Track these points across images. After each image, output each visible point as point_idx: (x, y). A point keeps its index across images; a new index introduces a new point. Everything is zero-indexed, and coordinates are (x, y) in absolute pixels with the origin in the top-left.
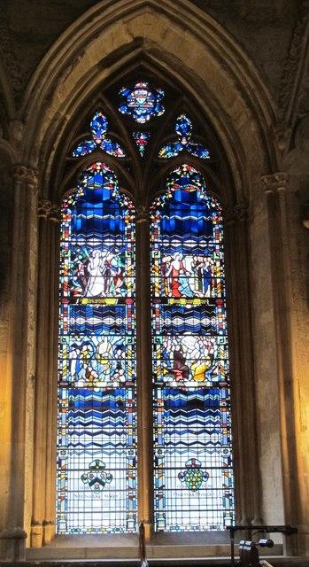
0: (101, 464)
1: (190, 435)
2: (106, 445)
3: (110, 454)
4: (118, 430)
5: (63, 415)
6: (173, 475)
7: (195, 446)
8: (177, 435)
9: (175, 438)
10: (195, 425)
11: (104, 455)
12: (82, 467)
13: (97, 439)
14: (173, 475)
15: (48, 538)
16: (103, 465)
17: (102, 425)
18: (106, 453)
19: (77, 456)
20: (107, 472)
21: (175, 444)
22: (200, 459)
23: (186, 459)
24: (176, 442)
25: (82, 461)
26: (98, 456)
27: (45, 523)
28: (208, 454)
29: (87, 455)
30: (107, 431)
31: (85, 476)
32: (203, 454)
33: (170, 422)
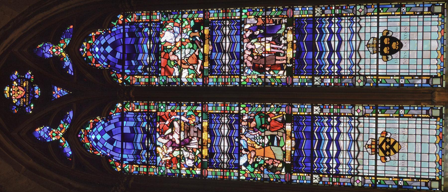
1: (342, 49)
3: (359, 133)
4: (335, 124)
8: (342, 63)
9: (345, 65)
10: (333, 43)
11: (361, 138)
17: (331, 140)
20: (379, 136)
22: (368, 38)
26: (360, 144)
28: (362, 30)
29: (360, 156)
30: (335, 135)
32: (362, 36)
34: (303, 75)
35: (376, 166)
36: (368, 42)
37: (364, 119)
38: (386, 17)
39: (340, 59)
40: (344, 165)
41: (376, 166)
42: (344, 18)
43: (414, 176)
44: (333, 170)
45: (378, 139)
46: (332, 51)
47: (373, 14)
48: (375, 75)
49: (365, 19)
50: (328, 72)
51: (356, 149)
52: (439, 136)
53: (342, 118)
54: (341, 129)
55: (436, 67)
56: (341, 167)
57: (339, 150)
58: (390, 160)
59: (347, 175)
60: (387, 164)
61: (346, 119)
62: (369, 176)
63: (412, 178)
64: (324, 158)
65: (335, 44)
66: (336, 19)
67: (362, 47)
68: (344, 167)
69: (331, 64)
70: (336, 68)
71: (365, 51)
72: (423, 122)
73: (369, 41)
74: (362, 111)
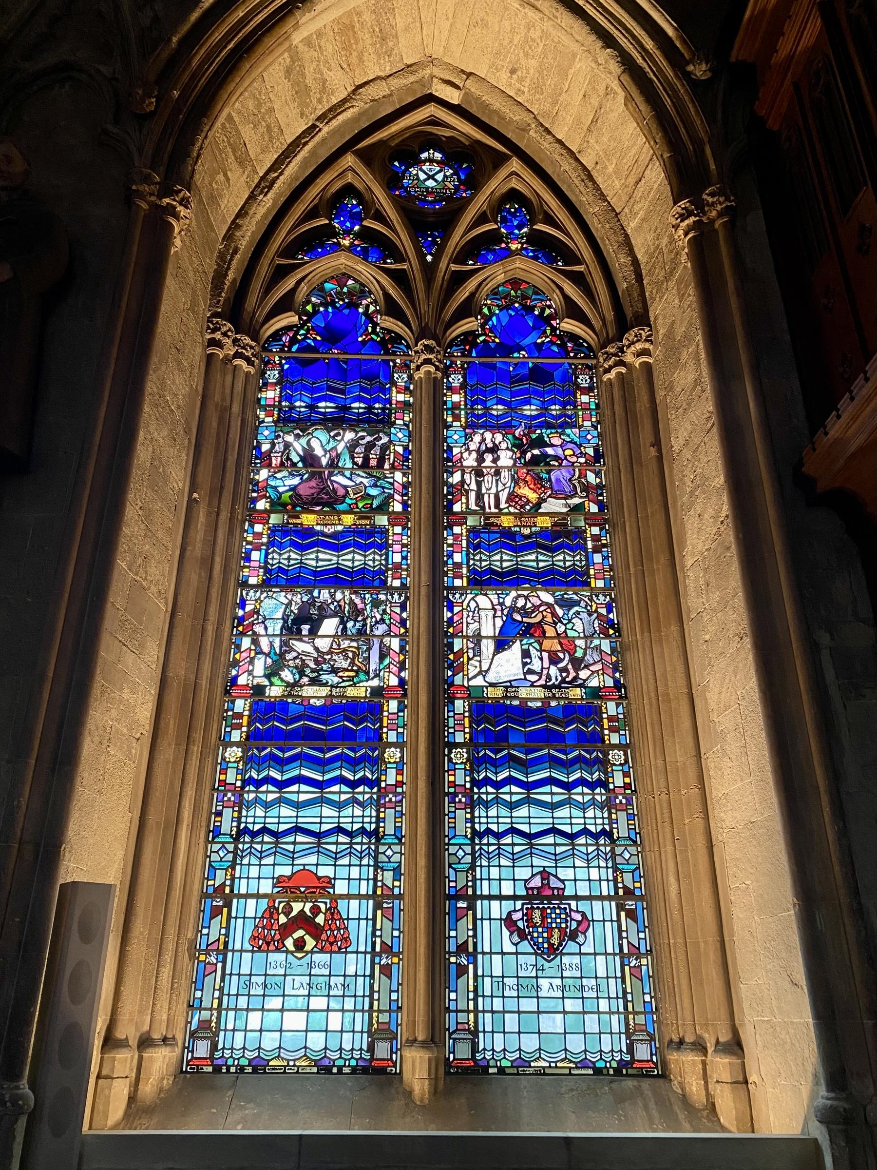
1: (535, 811)
2: (329, 833)
5: (234, 753)
6: (495, 914)
7: (549, 839)
10: (547, 789)
11: (323, 859)
14: (495, 914)
19: (254, 861)
21: (498, 836)
22: (562, 873)
23: (523, 873)
24: (502, 828)
25: (267, 871)
26: (313, 859)
27: (145, 1042)
29: (280, 859)
33: (487, 781)
34: (470, 723)
36: (553, 875)
37: (369, 865)
39: (512, 806)
40: (262, 820)
42: (606, 815)
43: (226, 991)
44: (253, 792)
46: (529, 786)
47: (620, 885)
48: (474, 891)
49: (607, 867)
50: (481, 778)
51: (299, 847)
52: (325, 1056)
53: (374, 814)
54: (348, 811)
55: (499, 1047)
56: (260, 812)
57: (298, 806)
59: (238, 827)
62: (233, 879)
63: (221, 989)
64: (282, 772)
65: (544, 794)
66: (604, 798)
67: (536, 861)
68: (257, 820)
69: (498, 785)
71: (532, 866)
72: (359, 1015)
73: (556, 876)
74: (390, 862)
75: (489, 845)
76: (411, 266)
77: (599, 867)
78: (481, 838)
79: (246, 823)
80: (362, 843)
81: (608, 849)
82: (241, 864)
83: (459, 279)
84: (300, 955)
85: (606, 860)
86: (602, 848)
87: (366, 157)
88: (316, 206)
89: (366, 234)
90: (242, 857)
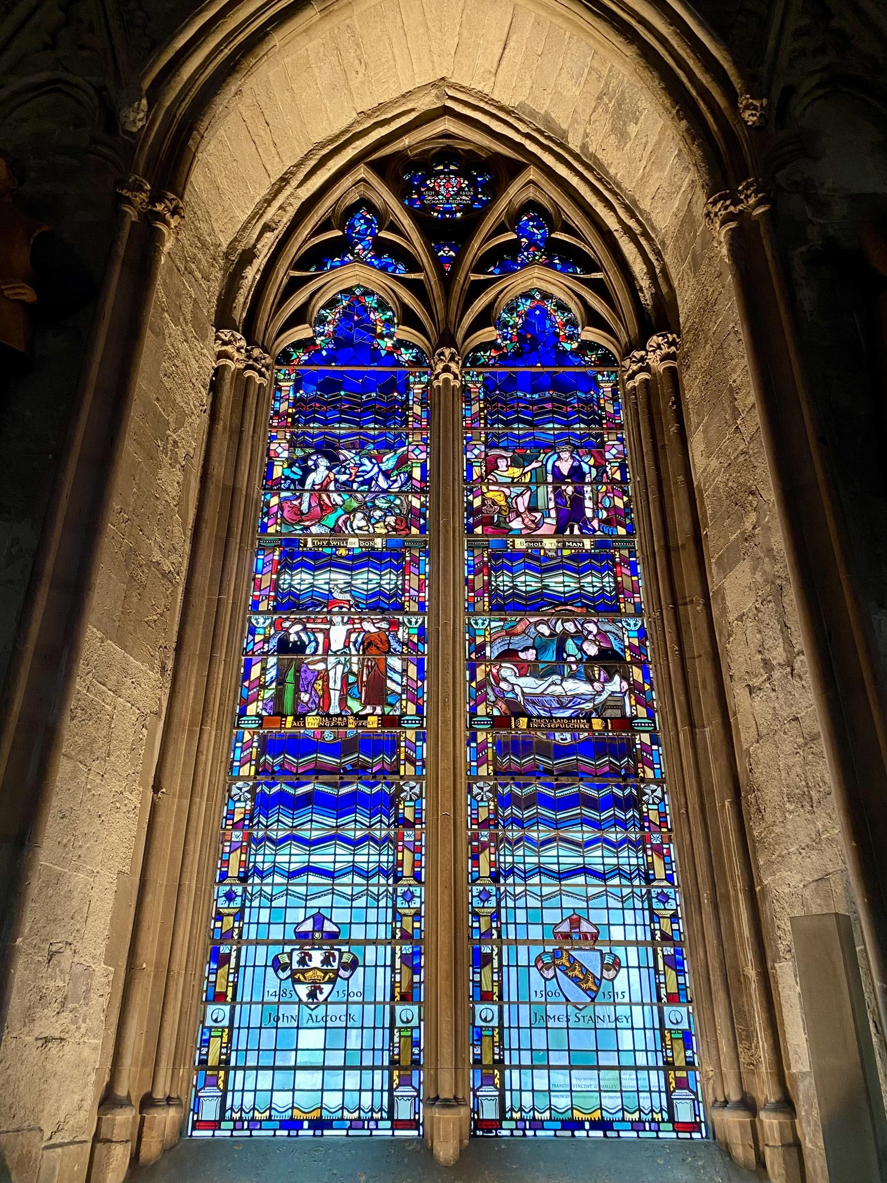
0: (328, 927)
7: (580, 880)
11: (340, 901)
12: (276, 933)
13: (322, 858)
14: (523, 961)
15: (151, 1148)
16: (335, 929)
18: (343, 895)
23: (552, 916)
26: (325, 901)
27: (148, 1102)
29: (292, 901)
31: (284, 959)
32: (600, 902)
35: (268, 943)
37: (387, 907)
38: (651, 965)
41: (268, 943)
45: (335, 947)
49: (643, 909)
58: (281, 980)
60: (270, 970)
61: (388, 862)
67: (567, 902)
70: (517, 835)
73: (588, 921)
75: (514, 885)
76: (429, 275)
77: (634, 909)
78: (506, 877)
79: (255, 862)
80: (378, 885)
81: (644, 891)
82: (251, 907)
83: (478, 289)
84: (312, 1006)
85: (643, 902)
86: (637, 890)
87: (381, 168)
88: (329, 219)
89: (380, 247)
90: (251, 901)
